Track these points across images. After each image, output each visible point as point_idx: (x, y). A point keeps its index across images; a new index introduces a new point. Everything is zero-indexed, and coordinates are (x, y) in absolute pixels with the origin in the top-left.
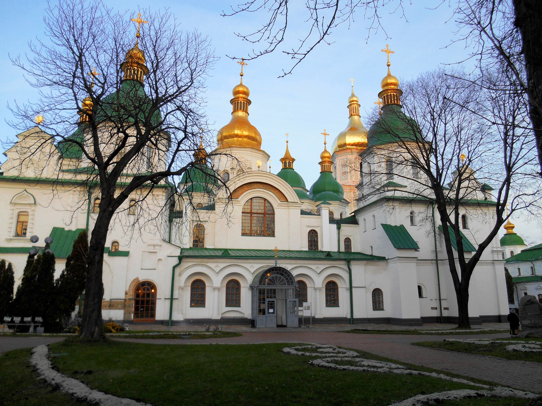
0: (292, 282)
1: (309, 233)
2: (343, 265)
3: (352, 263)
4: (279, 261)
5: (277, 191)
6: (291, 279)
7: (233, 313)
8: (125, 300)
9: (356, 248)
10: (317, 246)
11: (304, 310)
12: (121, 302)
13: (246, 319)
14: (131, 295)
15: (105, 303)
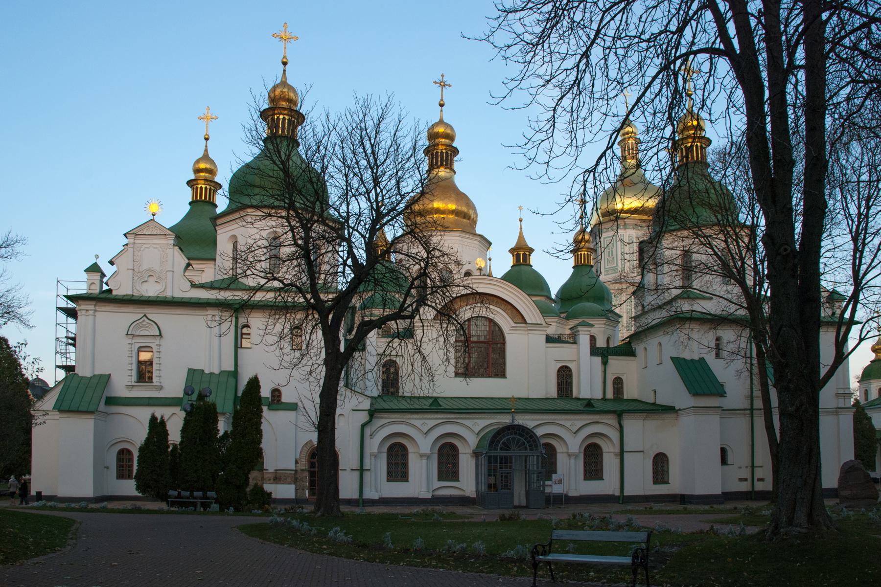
0: (536, 446)
1: (559, 371)
2: (612, 420)
3: (625, 416)
4: (517, 416)
5: (509, 307)
6: (535, 441)
7: (448, 489)
8: (296, 471)
9: (631, 392)
10: (571, 391)
11: (554, 486)
12: (291, 474)
13: (468, 498)
14: (304, 465)
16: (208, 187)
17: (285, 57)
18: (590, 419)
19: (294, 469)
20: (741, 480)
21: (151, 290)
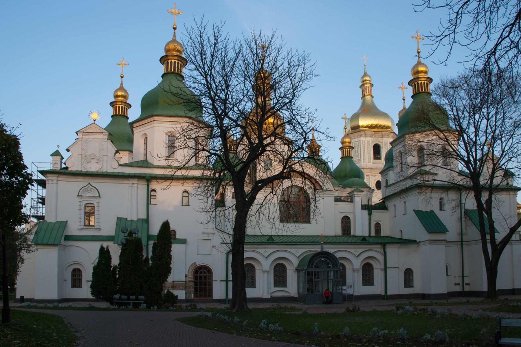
0: (337, 265)
1: (342, 219)
2: (379, 248)
3: (387, 246)
4: (325, 246)
6: (335, 262)
7: (280, 292)
8: (186, 282)
9: (385, 232)
10: (350, 231)
12: (183, 283)
14: (191, 278)
15: (169, 285)
16: (123, 106)
17: (175, 25)
18: (366, 248)
19: (185, 280)
20: (455, 284)
21: (93, 168)
